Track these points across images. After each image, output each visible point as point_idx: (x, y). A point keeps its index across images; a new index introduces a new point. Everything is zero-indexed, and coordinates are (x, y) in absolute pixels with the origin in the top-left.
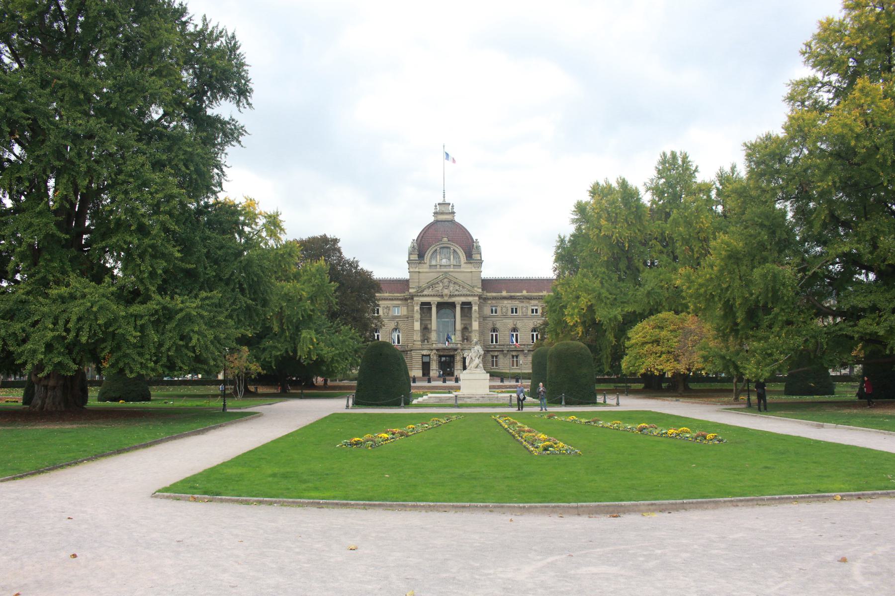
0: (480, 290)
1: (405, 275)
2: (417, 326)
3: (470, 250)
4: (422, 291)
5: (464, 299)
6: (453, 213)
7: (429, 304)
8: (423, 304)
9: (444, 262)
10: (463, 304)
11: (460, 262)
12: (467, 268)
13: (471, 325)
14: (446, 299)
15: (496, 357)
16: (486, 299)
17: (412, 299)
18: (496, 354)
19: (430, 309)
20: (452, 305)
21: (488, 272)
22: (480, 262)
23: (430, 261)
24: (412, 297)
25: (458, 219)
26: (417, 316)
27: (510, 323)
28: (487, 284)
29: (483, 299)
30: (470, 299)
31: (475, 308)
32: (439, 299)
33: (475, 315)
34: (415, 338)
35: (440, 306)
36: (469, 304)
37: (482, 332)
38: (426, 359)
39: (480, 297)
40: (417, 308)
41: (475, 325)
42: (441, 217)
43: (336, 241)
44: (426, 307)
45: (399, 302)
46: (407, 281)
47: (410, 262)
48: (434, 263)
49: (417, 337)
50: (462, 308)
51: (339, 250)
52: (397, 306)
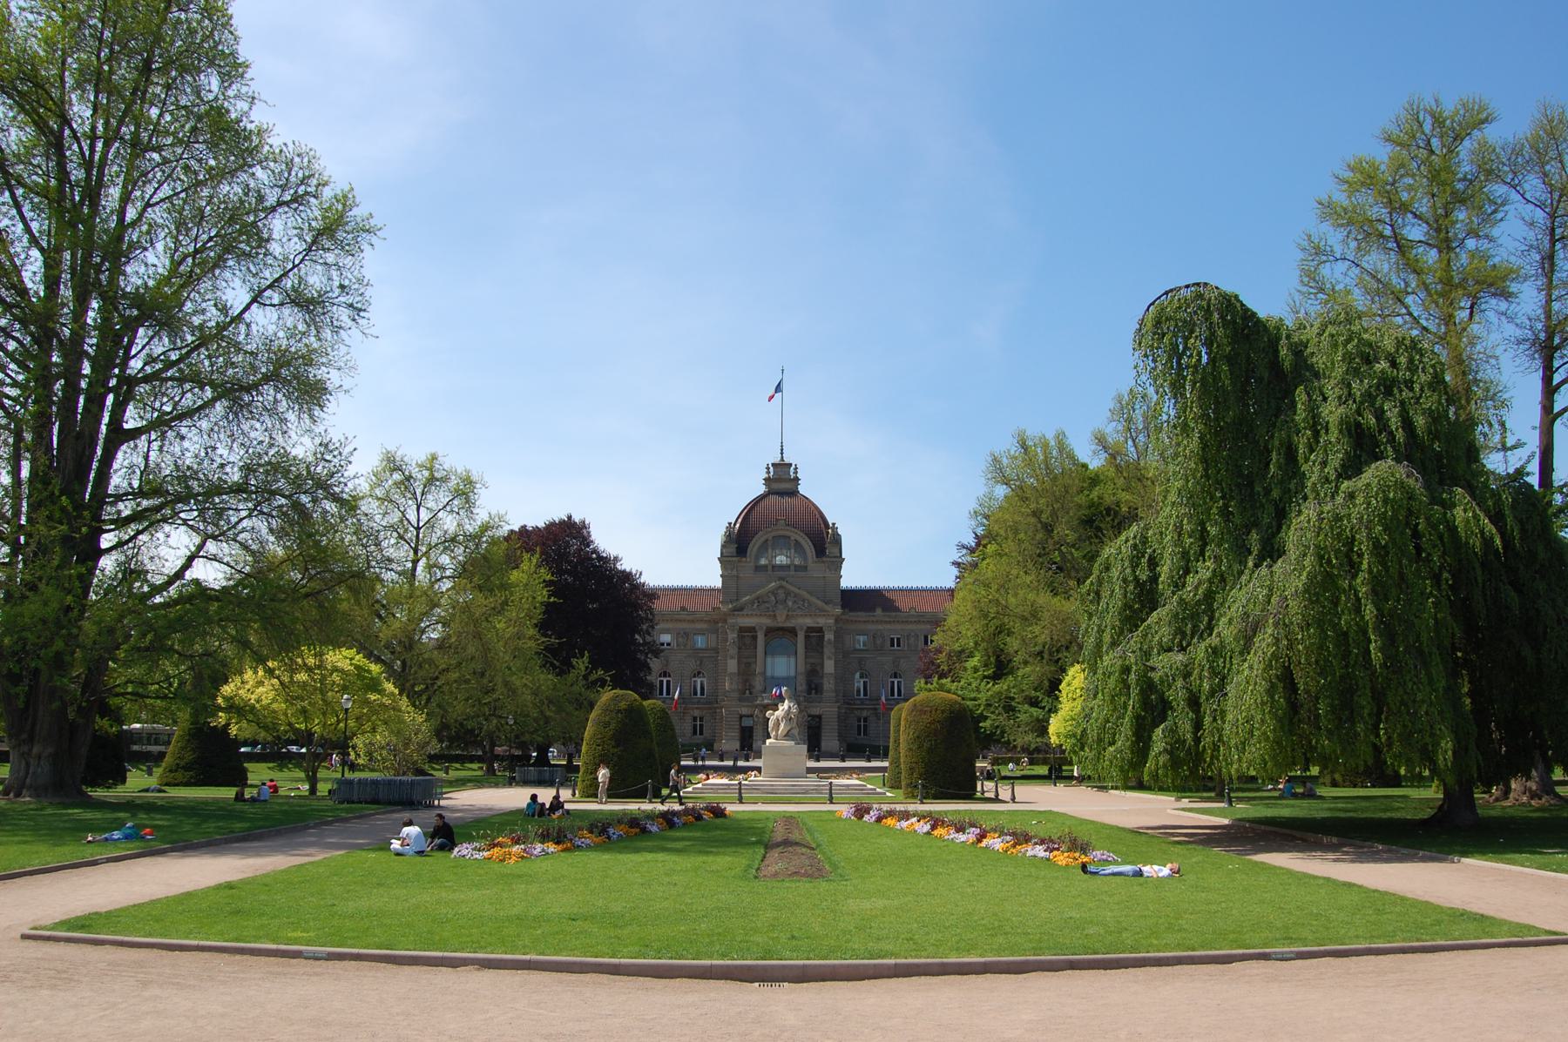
2: (732, 665)
3: (823, 541)
5: (809, 622)
6: (797, 479)
7: (752, 629)
8: (742, 630)
9: (781, 559)
10: (810, 629)
11: (805, 559)
12: (817, 570)
13: (822, 665)
14: (781, 621)
15: (865, 720)
17: (725, 621)
18: (865, 714)
19: (755, 638)
20: (793, 632)
21: (852, 577)
22: (838, 561)
23: (757, 558)
25: (802, 489)
30: (821, 622)
31: (829, 636)
33: (828, 651)
35: (771, 632)
36: (820, 630)
38: (747, 722)
40: (732, 636)
41: (829, 666)
42: (776, 486)
44: (747, 634)
45: (705, 626)
48: (763, 562)
50: (807, 637)
52: (701, 632)
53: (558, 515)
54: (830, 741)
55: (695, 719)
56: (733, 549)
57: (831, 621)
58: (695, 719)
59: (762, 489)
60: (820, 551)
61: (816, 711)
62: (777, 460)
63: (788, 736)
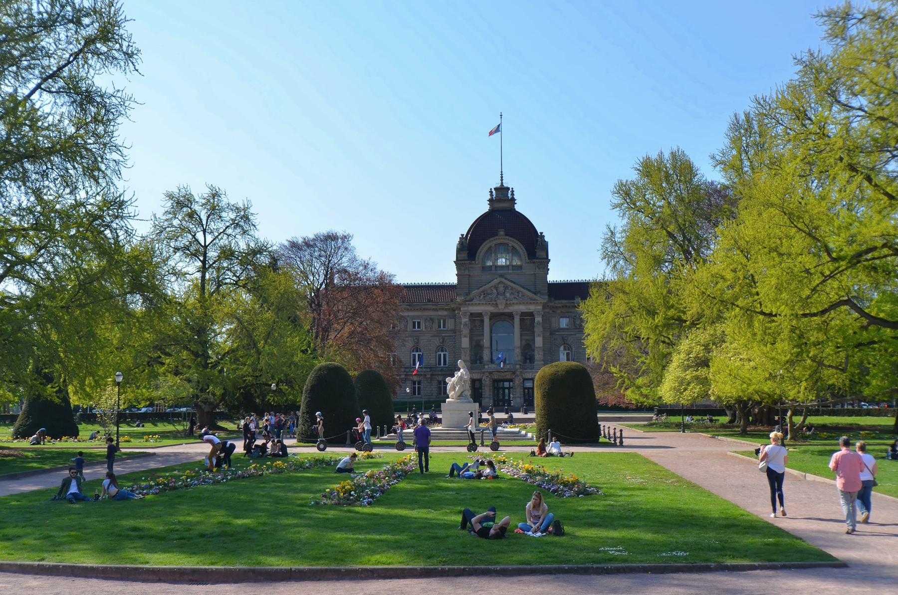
2: (465, 342)
3: (534, 246)
4: (472, 300)
5: (523, 308)
6: (513, 200)
7: (480, 315)
8: (472, 315)
10: (523, 314)
14: (501, 308)
19: (482, 321)
20: (511, 316)
23: (484, 262)
25: (518, 208)
26: (466, 331)
30: (532, 308)
31: (538, 319)
32: (491, 309)
33: (538, 330)
35: (494, 317)
36: (531, 314)
40: (465, 320)
41: (539, 342)
44: (477, 319)
50: (522, 320)
56: (465, 255)
57: (540, 307)
59: (485, 208)
62: (498, 185)
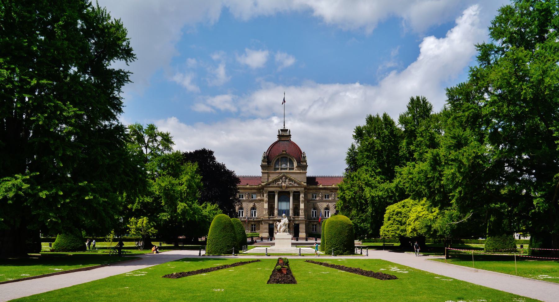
0: (305, 184)
1: (261, 175)
2: (266, 206)
5: (294, 189)
6: (290, 135)
7: (273, 192)
8: (270, 192)
9: (284, 166)
10: (295, 192)
11: (293, 166)
14: (284, 189)
15: (315, 225)
16: (309, 189)
17: (263, 189)
18: (315, 223)
20: (288, 193)
21: (310, 172)
22: (305, 167)
23: (275, 166)
24: (263, 188)
25: (292, 139)
27: (325, 205)
28: (312, 181)
29: (307, 190)
30: (299, 189)
32: (279, 189)
34: (264, 213)
37: (306, 210)
39: (305, 188)
41: (302, 206)
43: (211, 153)
45: (255, 191)
46: (261, 177)
47: (262, 166)
49: (265, 212)
51: (214, 158)
53: (200, 148)
54: (302, 234)
55: (252, 225)
57: (303, 189)
58: (252, 225)
59: (276, 139)
60: (299, 162)
61: (297, 222)
63: (284, 231)
